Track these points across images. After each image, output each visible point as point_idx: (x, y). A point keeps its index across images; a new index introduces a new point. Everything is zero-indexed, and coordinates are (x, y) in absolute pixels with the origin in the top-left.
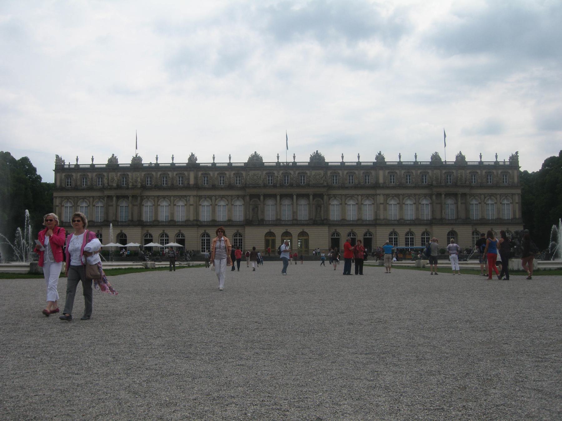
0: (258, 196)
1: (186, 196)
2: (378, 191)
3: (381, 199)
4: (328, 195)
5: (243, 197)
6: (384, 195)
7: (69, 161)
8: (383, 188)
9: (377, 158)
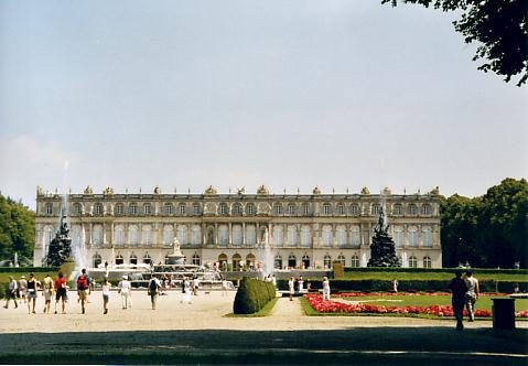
0: (213, 224)
1: (152, 223)
2: (315, 220)
3: (317, 227)
5: (201, 224)
7: (49, 192)
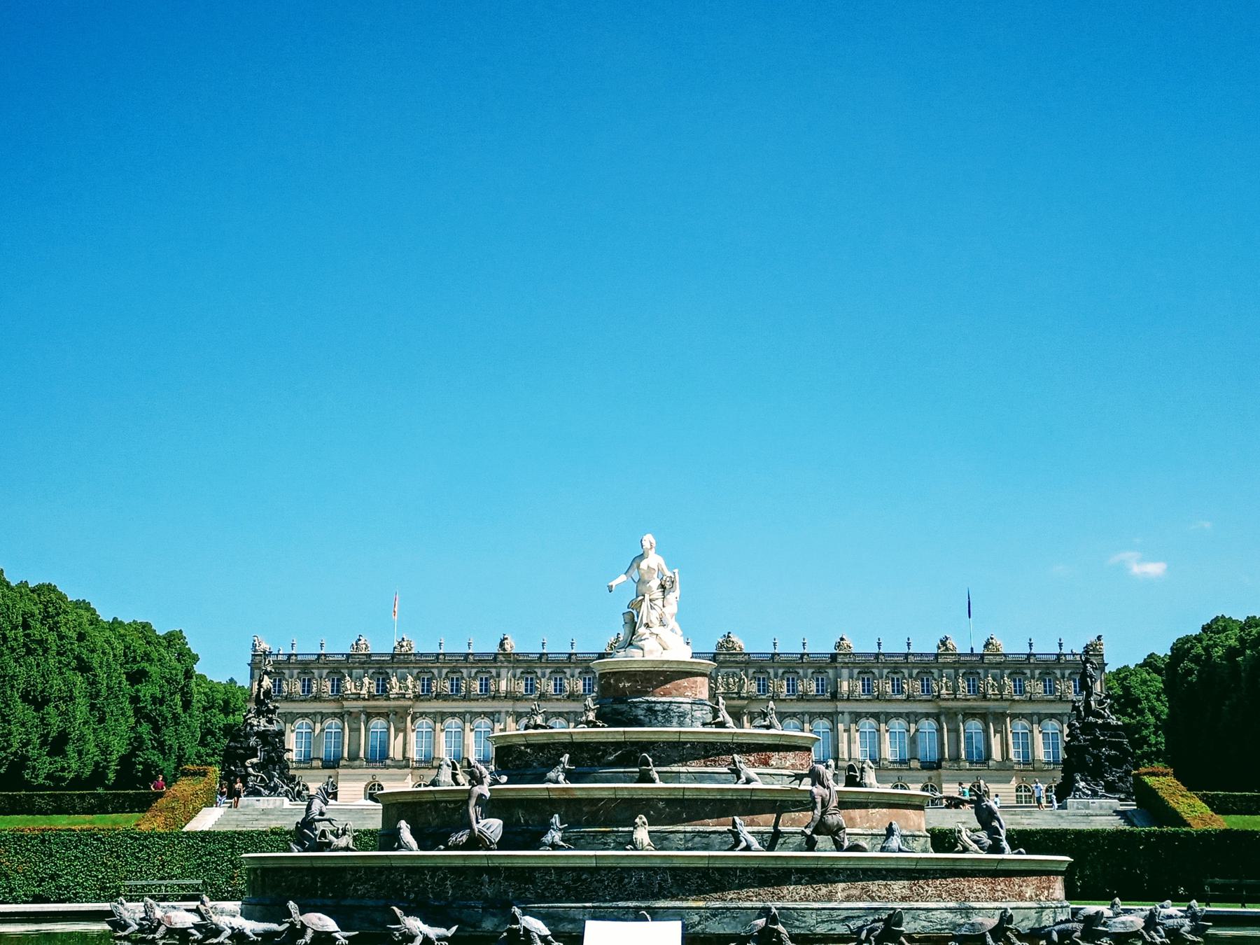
2: (841, 706)
4: (750, 713)
6: (850, 713)
7: (277, 644)
8: (848, 699)
9: (838, 646)
